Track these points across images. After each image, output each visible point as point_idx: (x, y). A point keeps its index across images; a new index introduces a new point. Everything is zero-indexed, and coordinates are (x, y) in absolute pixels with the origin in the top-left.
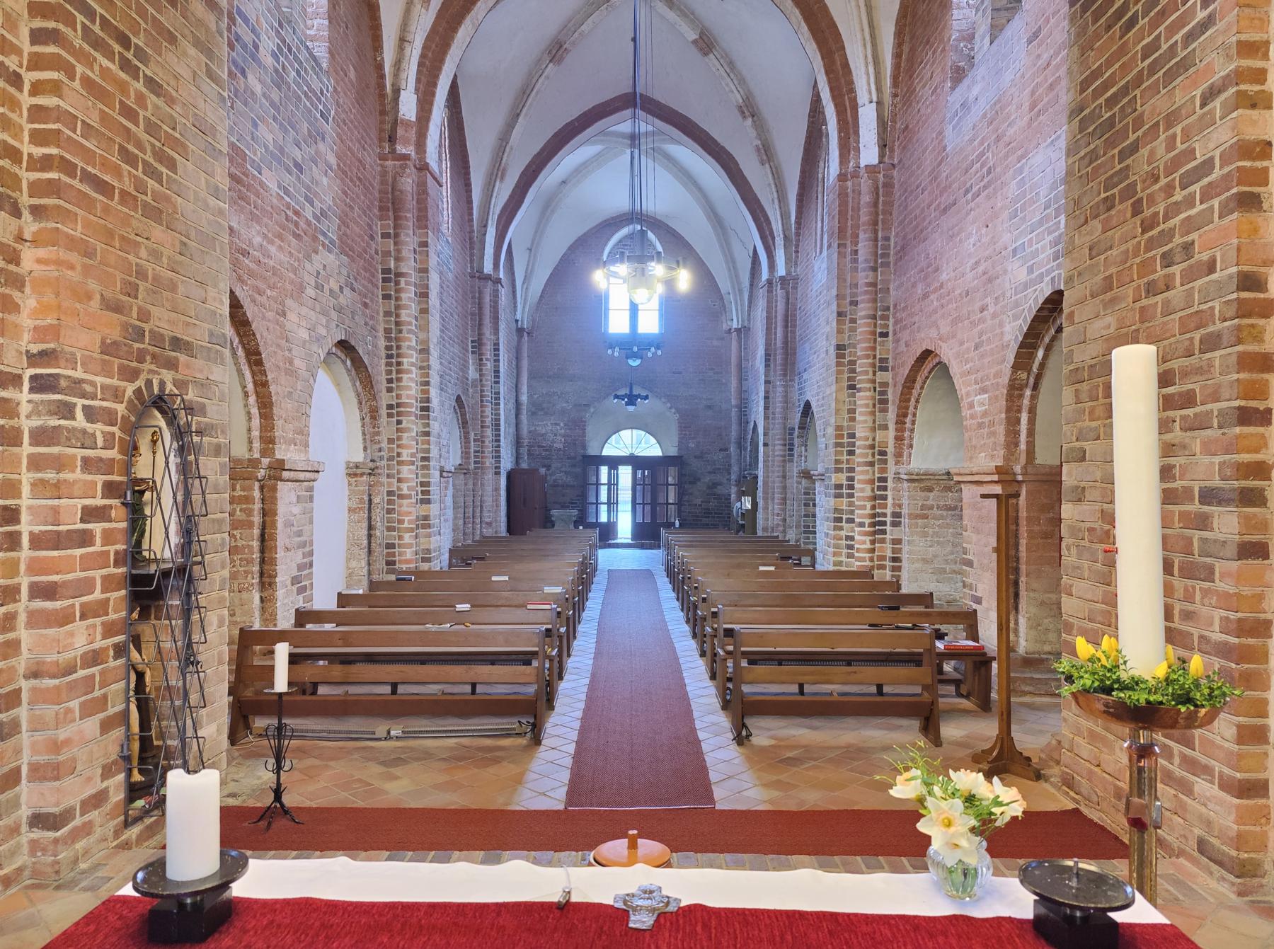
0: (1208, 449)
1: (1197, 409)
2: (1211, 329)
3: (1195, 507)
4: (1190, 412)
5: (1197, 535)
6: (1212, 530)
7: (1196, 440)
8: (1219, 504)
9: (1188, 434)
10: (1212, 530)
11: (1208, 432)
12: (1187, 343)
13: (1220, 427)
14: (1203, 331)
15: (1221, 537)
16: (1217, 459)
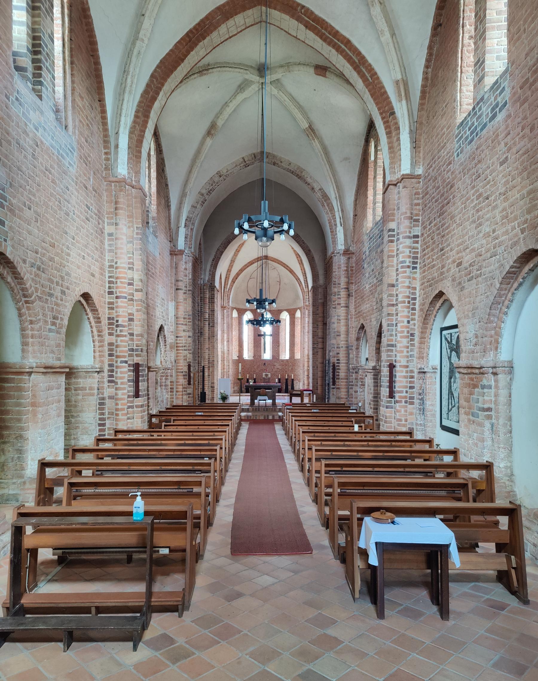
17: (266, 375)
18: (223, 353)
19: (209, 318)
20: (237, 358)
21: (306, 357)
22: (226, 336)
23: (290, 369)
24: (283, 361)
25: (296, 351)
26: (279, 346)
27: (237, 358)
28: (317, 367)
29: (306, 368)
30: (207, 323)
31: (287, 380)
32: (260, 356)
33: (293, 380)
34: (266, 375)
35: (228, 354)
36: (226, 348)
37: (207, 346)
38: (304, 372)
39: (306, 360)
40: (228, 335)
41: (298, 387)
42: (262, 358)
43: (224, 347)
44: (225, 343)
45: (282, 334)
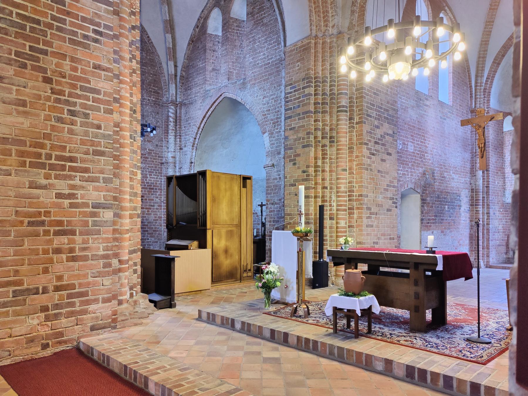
0: (96, 189)
1: (90, 174)
2: (99, 148)
3: (90, 209)
4: (86, 175)
5: (90, 220)
6: (100, 217)
7: (90, 186)
8: (104, 208)
9: (84, 183)
10: (100, 217)
11: (98, 184)
12: (86, 150)
13: (104, 183)
14: (94, 148)
15: (104, 219)
16: (102, 194)
18: (474, 191)
19: (351, 106)
30: (344, 117)
36: (480, 182)
37: (344, 163)
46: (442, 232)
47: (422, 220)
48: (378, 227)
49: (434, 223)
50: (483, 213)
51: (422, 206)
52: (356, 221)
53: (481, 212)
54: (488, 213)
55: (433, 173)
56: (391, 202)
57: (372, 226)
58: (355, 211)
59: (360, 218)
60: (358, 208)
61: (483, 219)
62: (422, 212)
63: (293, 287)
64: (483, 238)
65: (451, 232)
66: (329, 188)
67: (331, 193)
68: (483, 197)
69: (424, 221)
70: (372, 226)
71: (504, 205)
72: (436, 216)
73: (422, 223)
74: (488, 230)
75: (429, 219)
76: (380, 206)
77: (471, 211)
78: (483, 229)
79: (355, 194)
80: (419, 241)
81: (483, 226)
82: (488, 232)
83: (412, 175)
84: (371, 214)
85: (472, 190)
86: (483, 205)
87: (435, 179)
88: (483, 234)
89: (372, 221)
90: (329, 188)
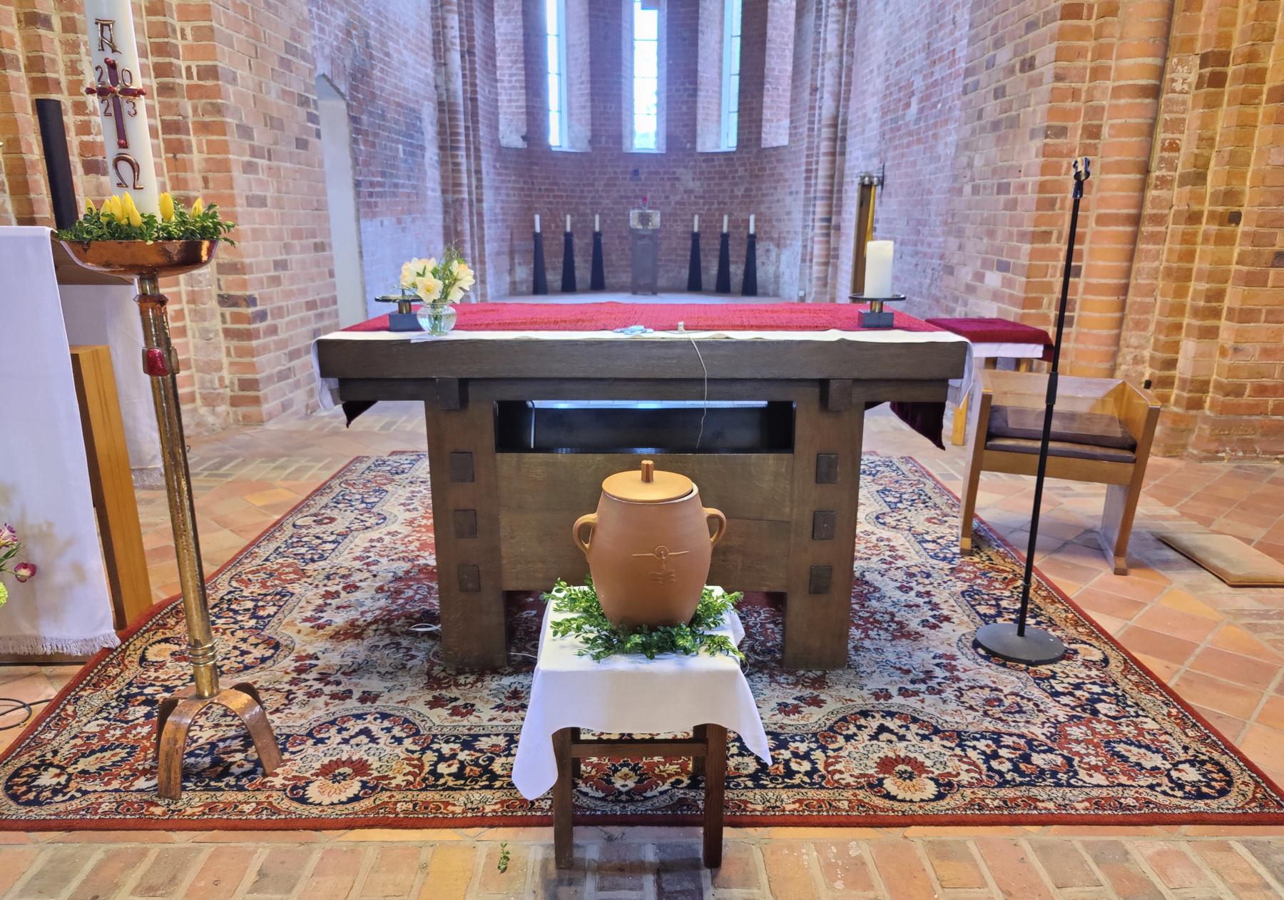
17: (644, 219)
18: (445, 108)
20: (520, 144)
21: (826, 132)
22: (454, 21)
23: (740, 191)
24: (710, 157)
25: (767, 114)
26: (694, 93)
27: (520, 144)
28: (1093, 132)
29: (821, 183)
31: (725, 238)
32: (618, 139)
33: (752, 240)
34: (644, 219)
35: (473, 115)
36: (458, 84)
38: (809, 202)
39: (824, 146)
40: (467, 23)
41: (771, 269)
42: (626, 148)
43: (448, 78)
44: (455, 58)
45: (707, 40)
46: (399, 221)
47: (357, 184)
48: (279, 204)
49: (381, 195)
50: (469, 171)
51: (355, 141)
52: (206, 180)
53: (464, 168)
54: (478, 172)
55: (367, 36)
56: (302, 112)
57: (262, 202)
58: (193, 139)
59: (224, 166)
60: (204, 128)
61: (470, 186)
62: (356, 161)
63: (80, 572)
64: (472, 235)
65: (414, 220)
66: (56, 22)
67: (73, 47)
68: (467, 128)
69: (364, 190)
70: (262, 202)
71: (501, 153)
72: (383, 174)
73: (358, 194)
74: (480, 214)
75: (372, 184)
76: (273, 123)
77: (443, 163)
78: (471, 214)
79: (183, 64)
80: (356, 250)
81: (471, 205)
82: (481, 221)
83: (322, 30)
84: (254, 152)
85: (441, 104)
86: (468, 149)
87: (371, 57)
88: (472, 227)
89: (261, 183)
90: (56, 22)
